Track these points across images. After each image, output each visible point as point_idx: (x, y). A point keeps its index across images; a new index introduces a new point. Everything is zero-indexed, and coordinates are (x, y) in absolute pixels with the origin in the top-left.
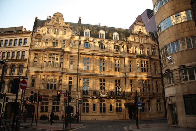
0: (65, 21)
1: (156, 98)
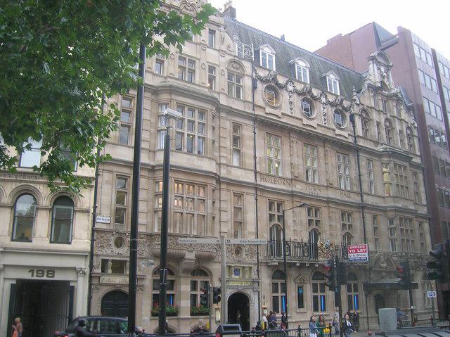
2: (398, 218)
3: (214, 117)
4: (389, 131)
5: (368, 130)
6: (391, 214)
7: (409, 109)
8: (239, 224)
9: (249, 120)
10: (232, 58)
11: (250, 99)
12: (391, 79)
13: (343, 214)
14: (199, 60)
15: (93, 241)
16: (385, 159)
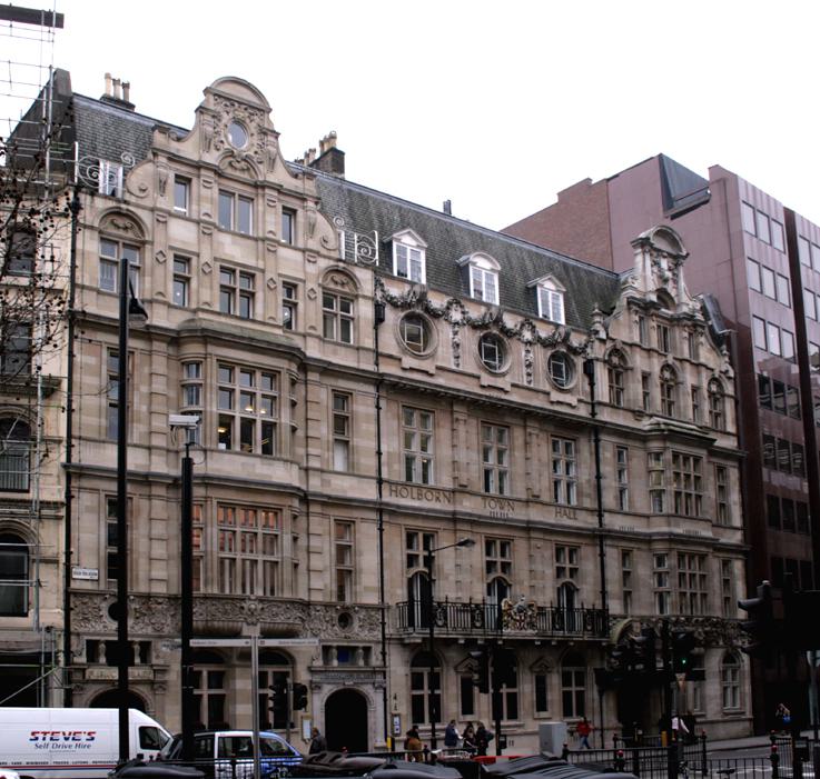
1: (721, 643)
2: (675, 553)
3: (293, 383)
4: (669, 388)
5: (622, 390)
6: (659, 547)
7: (718, 341)
8: (344, 576)
9: (366, 383)
10: (332, 263)
11: (369, 343)
12: (682, 284)
13: (559, 551)
14: (263, 271)
15: (68, 610)
16: (655, 446)
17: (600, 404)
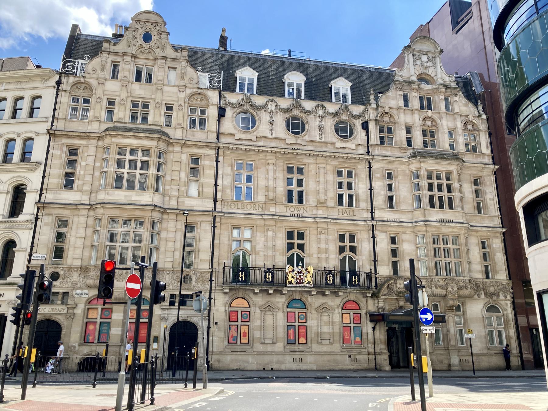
0: (173, 40)
17: (372, 145)
